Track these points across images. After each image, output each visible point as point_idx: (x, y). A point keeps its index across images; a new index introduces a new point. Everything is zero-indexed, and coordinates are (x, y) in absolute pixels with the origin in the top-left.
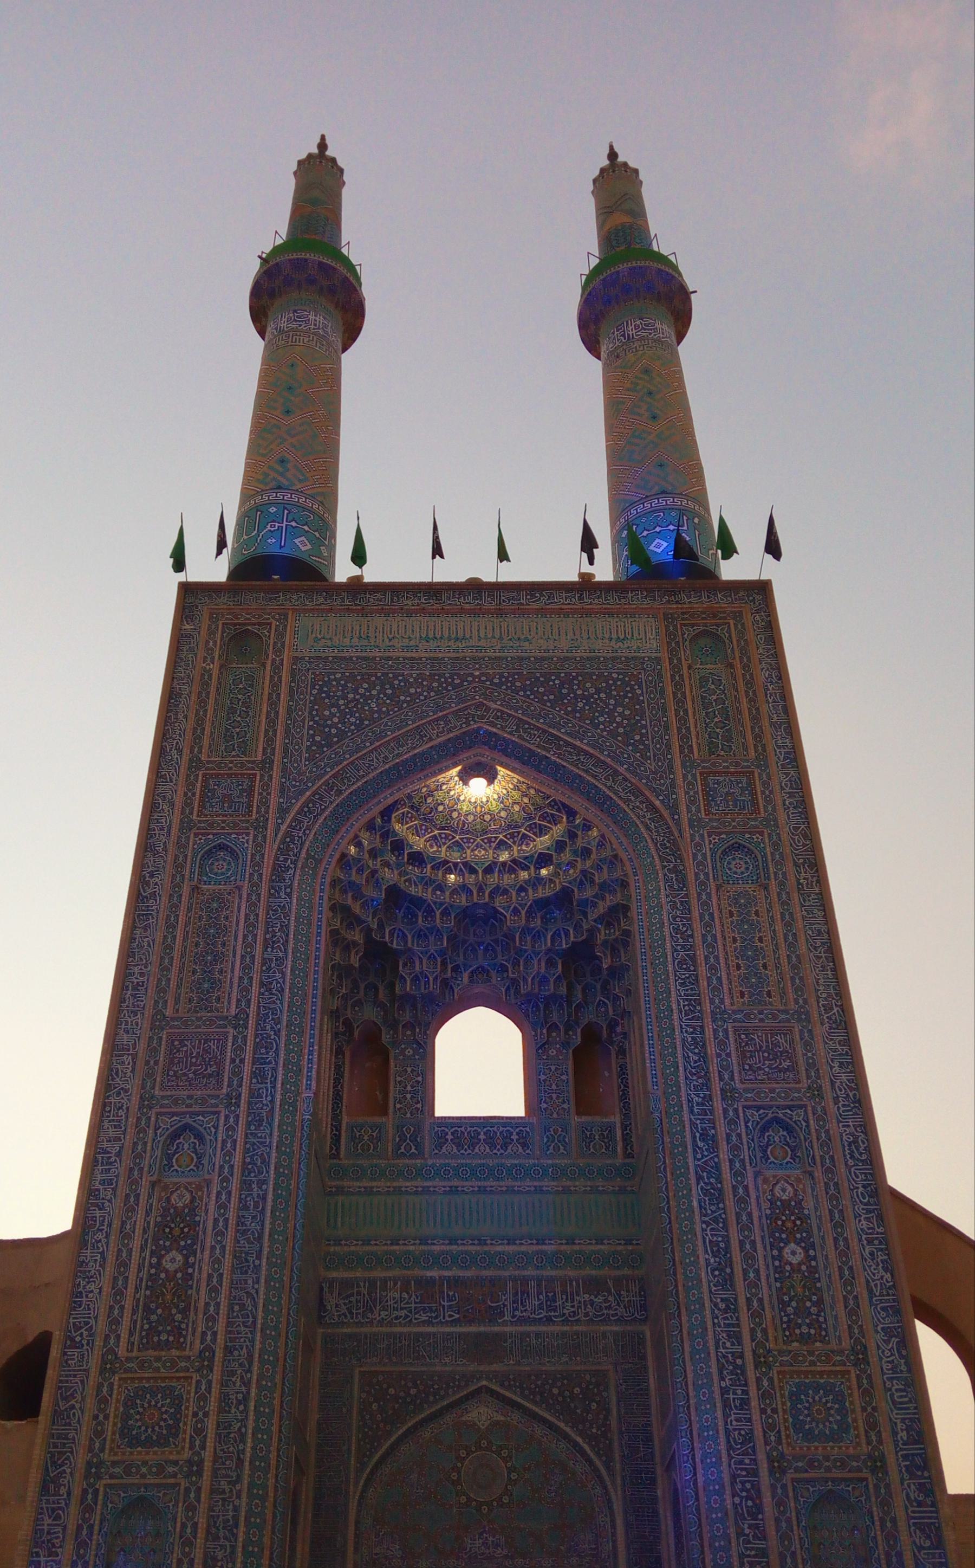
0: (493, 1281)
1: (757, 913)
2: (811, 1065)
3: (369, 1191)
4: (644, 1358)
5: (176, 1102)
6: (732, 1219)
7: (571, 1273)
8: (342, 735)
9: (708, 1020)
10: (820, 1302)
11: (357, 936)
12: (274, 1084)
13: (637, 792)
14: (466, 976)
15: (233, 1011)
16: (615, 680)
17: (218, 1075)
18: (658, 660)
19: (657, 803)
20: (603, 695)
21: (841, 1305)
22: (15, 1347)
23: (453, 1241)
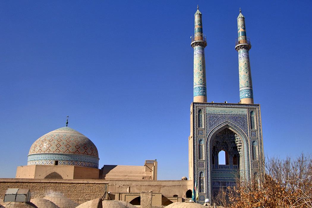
0: (226, 182)
13: (244, 134)
17: (204, 166)
23: (221, 178)
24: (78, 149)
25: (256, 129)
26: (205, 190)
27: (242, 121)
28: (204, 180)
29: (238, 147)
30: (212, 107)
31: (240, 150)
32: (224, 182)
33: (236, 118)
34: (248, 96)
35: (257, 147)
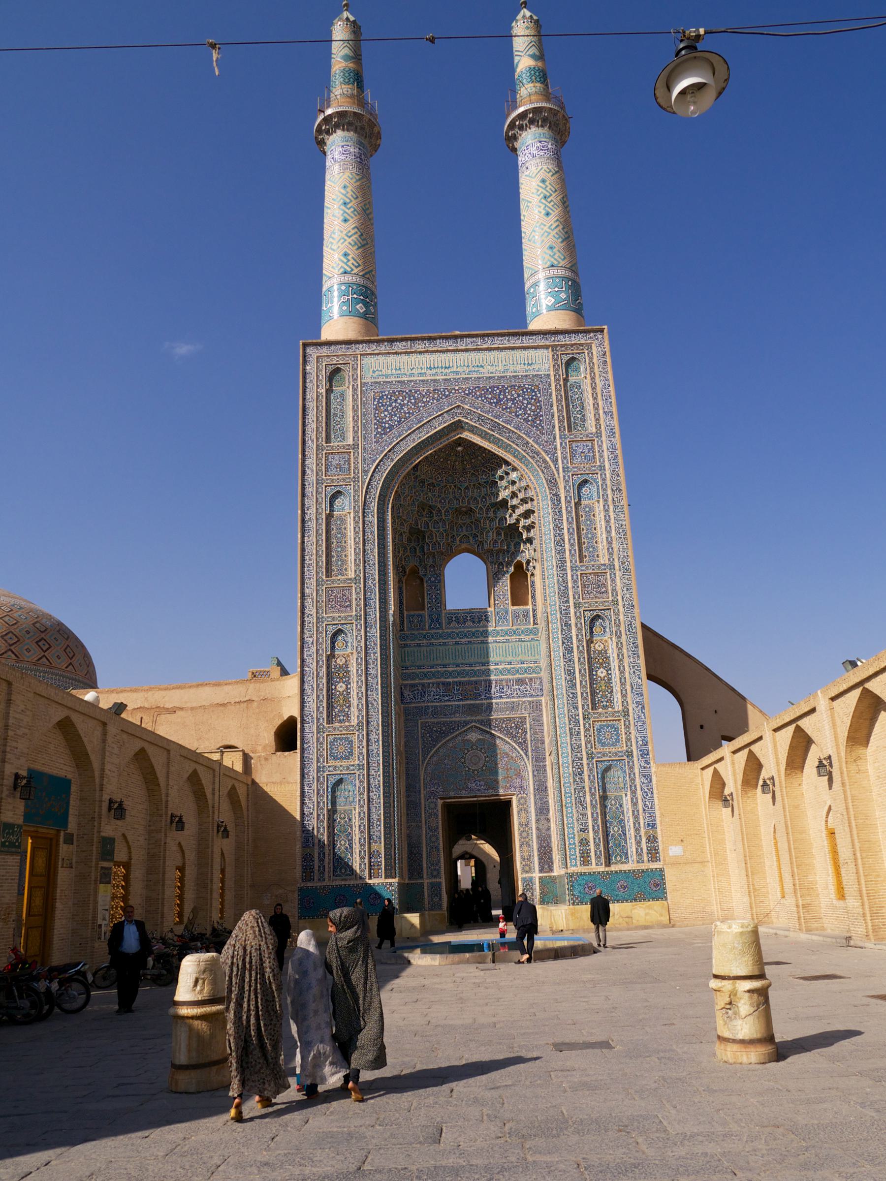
0: (476, 682)
1: (594, 515)
2: (614, 590)
3: (419, 645)
4: (541, 710)
5: (333, 618)
6: (576, 660)
7: (510, 677)
8: (391, 427)
9: (569, 571)
10: (612, 691)
11: (406, 529)
12: (375, 608)
13: (538, 454)
14: (458, 539)
15: (353, 576)
16: (527, 389)
17: (350, 606)
18: (549, 375)
19: (548, 459)
20: (521, 398)
21: (619, 694)
22: (280, 722)
23: (458, 666)
24: (11, 645)
25: (594, 430)
26: (354, 711)
27: (529, 403)
28: (351, 668)
29: (522, 523)
30: (392, 356)
31: (532, 534)
32: (469, 683)
33: (496, 392)
34: (554, 304)
35: (602, 507)
